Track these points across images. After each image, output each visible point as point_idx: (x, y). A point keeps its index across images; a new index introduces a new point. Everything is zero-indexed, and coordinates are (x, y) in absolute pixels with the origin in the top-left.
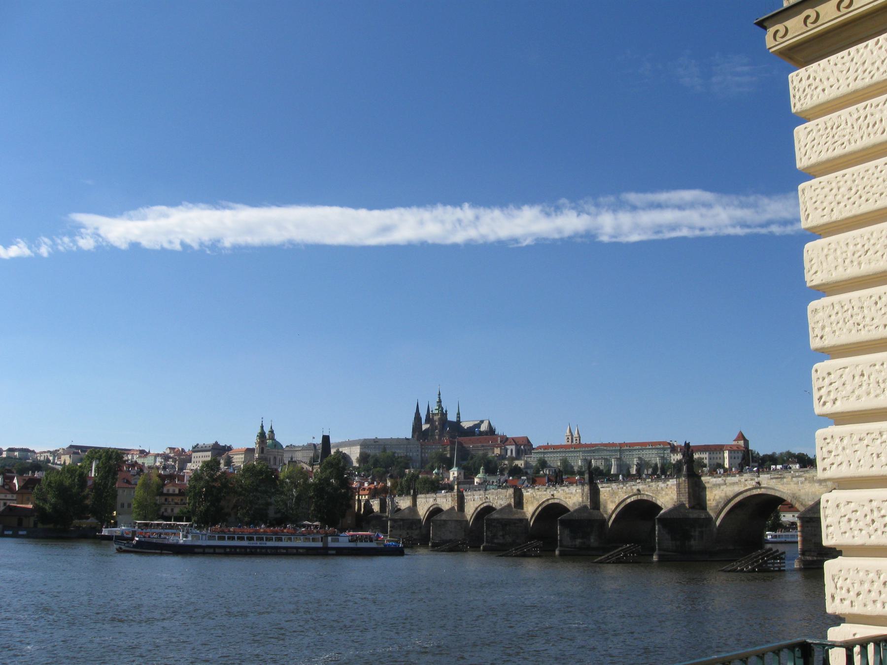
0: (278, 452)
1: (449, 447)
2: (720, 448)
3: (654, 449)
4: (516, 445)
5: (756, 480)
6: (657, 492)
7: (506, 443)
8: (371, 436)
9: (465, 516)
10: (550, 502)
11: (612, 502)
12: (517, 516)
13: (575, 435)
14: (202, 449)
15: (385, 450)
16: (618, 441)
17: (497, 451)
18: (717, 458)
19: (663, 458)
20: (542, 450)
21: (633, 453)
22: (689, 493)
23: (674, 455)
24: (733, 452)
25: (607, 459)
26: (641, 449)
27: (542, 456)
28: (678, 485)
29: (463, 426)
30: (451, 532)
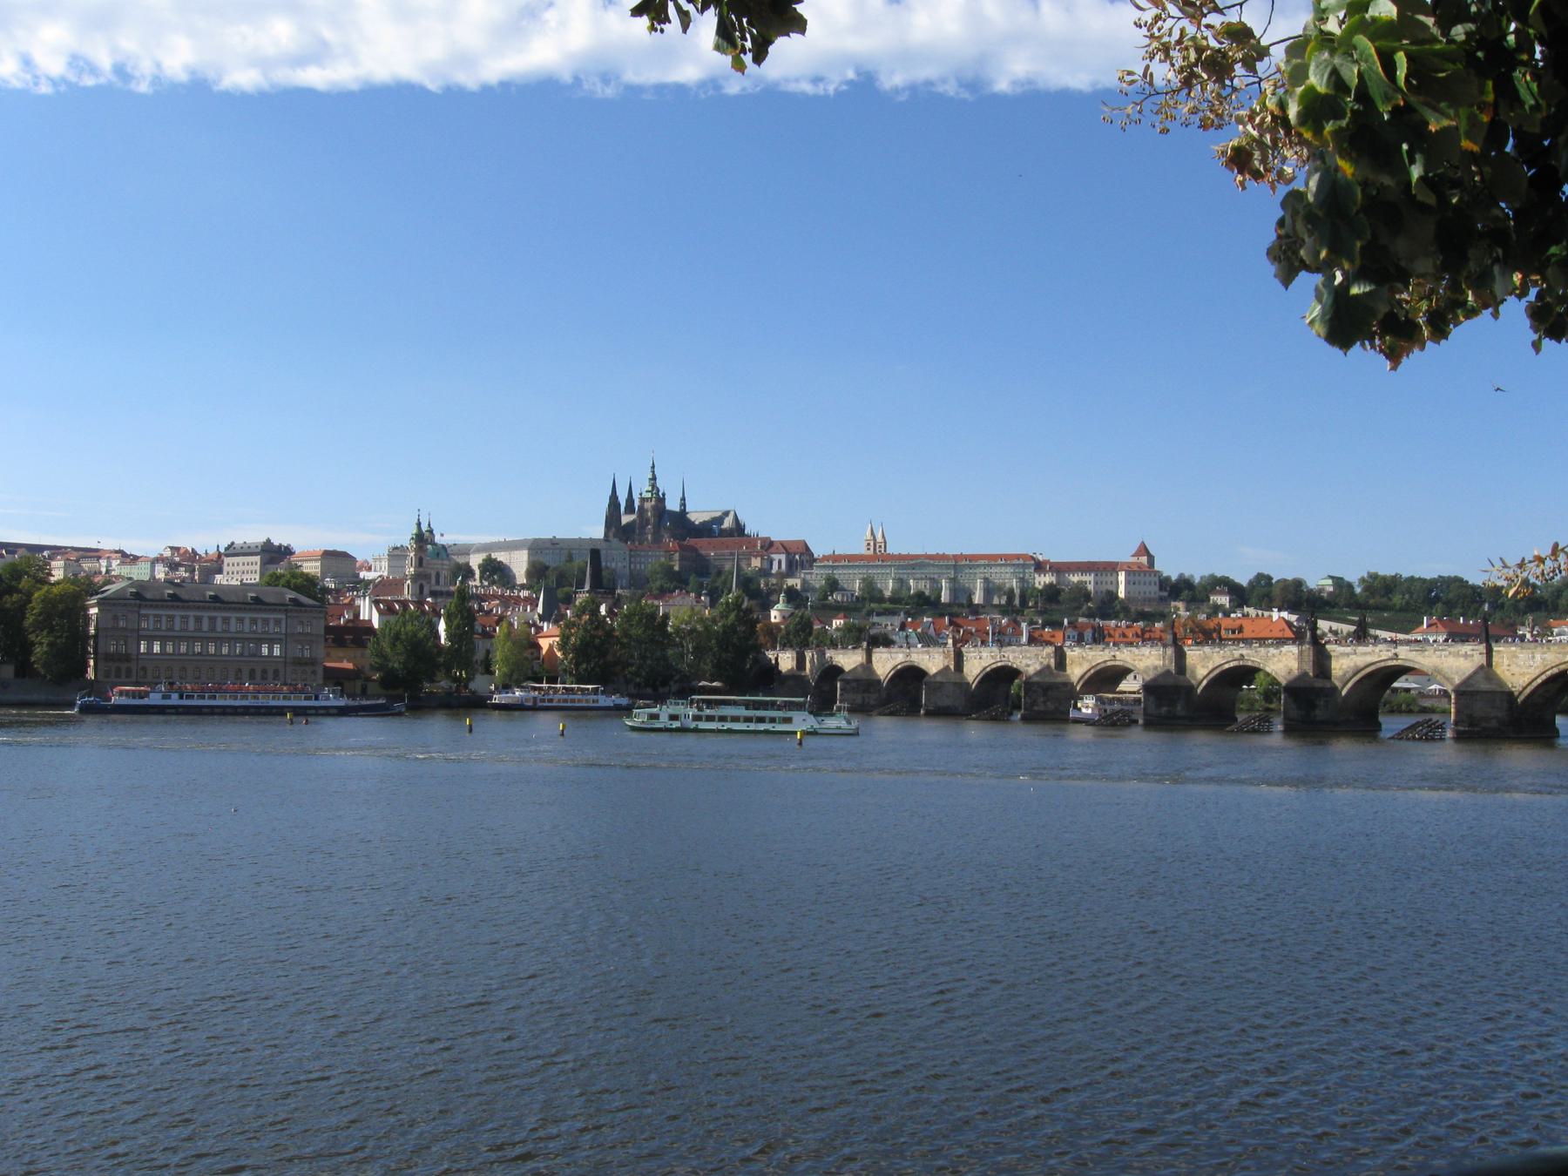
0: (442, 564)
1: (677, 554)
2: (1111, 568)
3: (1009, 565)
4: (788, 553)
5: (1393, 651)
6: (1267, 658)
8: (546, 534)
9: (963, 678)
10: (1109, 664)
11: (1203, 667)
12: (1059, 680)
13: (879, 538)
14: (249, 551)
15: (570, 558)
16: (950, 552)
17: (756, 563)
19: (1022, 580)
22: (1314, 662)
26: (988, 565)
28: (1301, 653)
29: (693, 520)
30: (948, 697)
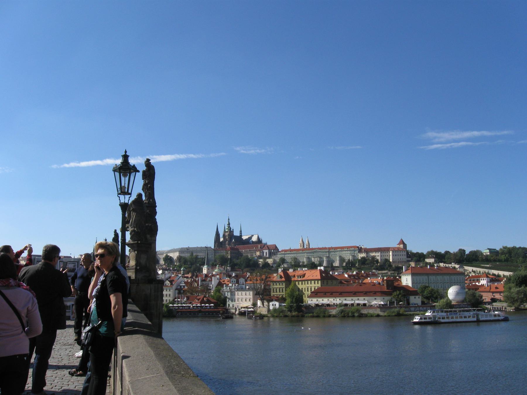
1: (230, 251)
2: (387, 250)
7: (263, 249)
8: (186, 246)
13: (306, 243)
16: (328, 246)
17: (258, 253)
18: (385, 256)
19: (354, 256)
20: (284, 253)
21: (336, 253)
23: (360, 254)
24: (395, 252)
25: (321, 257)
26: (341, 251)
27: (284, 256)
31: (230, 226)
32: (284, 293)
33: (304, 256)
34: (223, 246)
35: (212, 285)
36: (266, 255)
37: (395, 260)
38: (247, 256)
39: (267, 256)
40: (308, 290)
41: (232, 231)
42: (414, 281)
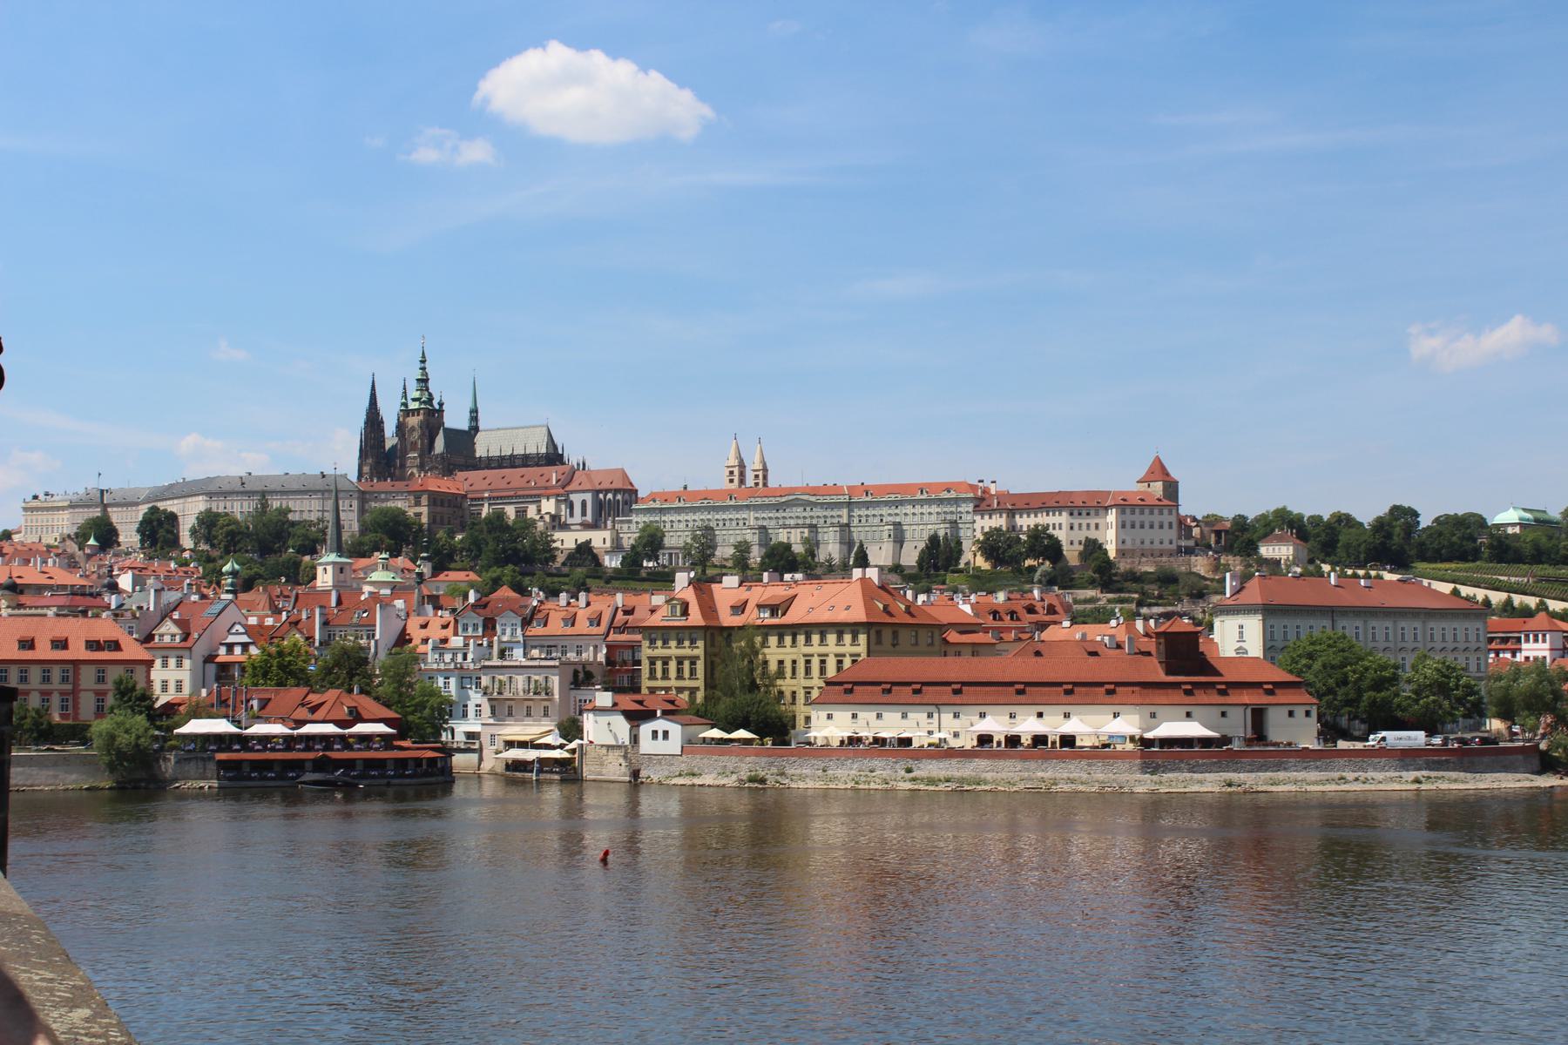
13: (753, 464)
20: (657, 505)
23: (982, 518)
25: (815, 526)
27: (657, 519)
31: (427, 389)
32: (700, 683)
33: (744, 519)
34: (397, 472)
35: (373, 642)
36: (584, 513)
37: (1129, 545)
38: (500, 516)
39: (589, 518)
40: (808, 671)
41: (437, 407)
42: (1272, 639)
